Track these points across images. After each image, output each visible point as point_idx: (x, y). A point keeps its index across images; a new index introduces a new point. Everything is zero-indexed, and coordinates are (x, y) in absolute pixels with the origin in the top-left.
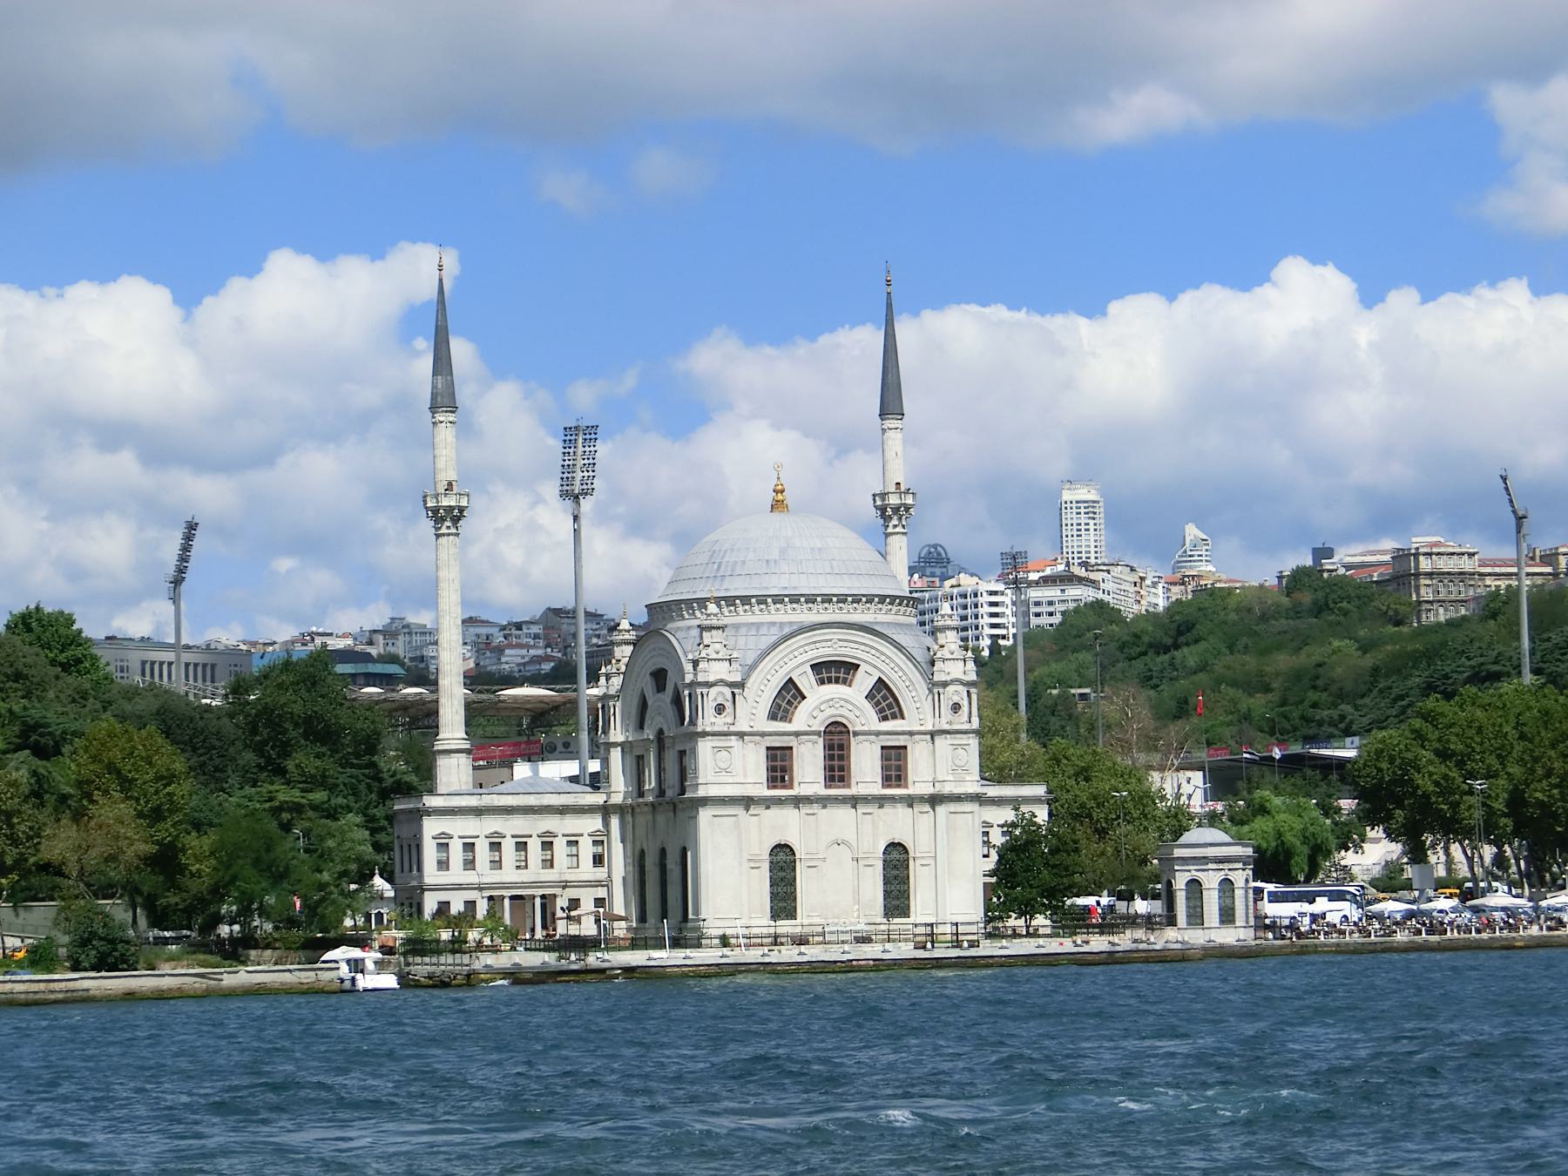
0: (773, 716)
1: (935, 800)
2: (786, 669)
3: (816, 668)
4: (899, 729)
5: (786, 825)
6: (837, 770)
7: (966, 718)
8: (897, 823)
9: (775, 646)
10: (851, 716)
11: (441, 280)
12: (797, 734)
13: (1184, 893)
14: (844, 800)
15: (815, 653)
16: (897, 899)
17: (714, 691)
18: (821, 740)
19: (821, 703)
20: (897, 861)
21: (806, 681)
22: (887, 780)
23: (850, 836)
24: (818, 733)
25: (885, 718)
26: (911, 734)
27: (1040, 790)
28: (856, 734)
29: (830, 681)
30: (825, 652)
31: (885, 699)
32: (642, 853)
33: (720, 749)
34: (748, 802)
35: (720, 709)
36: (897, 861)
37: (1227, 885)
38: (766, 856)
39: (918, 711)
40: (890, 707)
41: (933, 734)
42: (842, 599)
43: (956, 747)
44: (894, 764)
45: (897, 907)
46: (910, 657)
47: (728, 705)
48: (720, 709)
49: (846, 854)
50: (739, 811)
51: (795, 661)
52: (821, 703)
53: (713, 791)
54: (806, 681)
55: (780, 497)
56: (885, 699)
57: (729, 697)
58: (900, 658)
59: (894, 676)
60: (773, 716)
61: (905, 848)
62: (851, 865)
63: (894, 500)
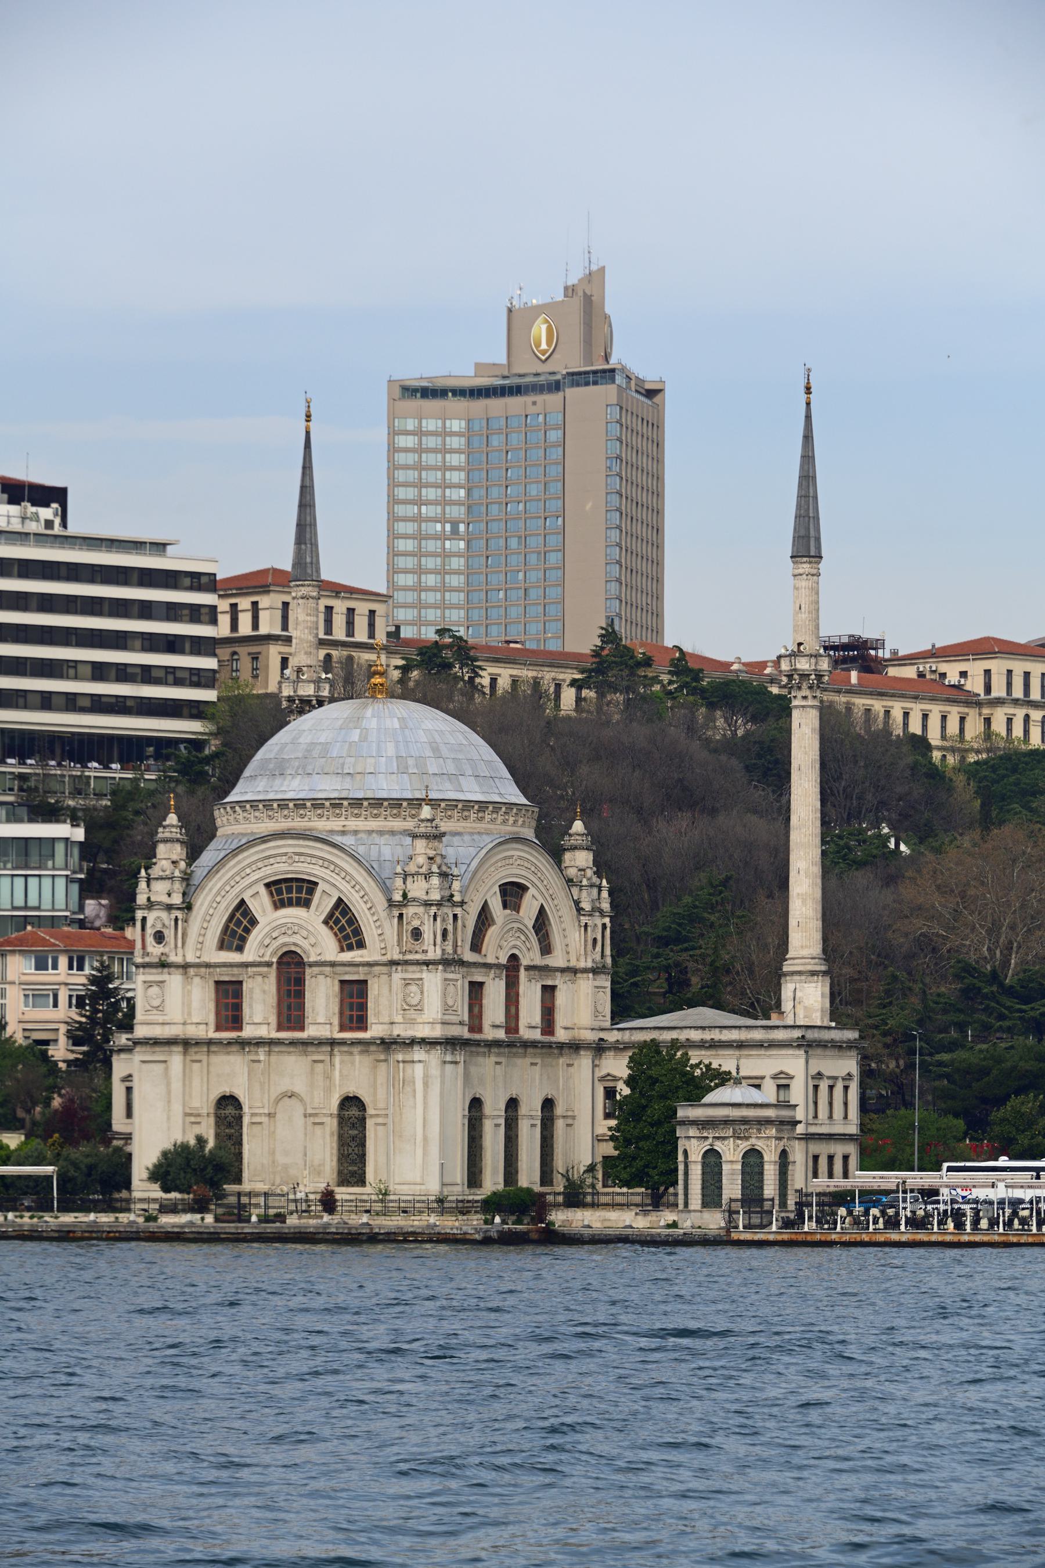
0: (222, 946)
1: (388, 1044)
2: (237, 889)
3: (268, 885)
4: (358, 959)
6: (291, 1008)
9: (221, 863)
10: (304, 944)
11: (308, 433)
12: (246, 965)
13: (699, 1167)
14: (293, 1043)
15: (268, 870)
16: (352, 1164)
18: (273, 972)
19: (275, 927)
21: (260, 905)
23: (299, 1087)
24: (269, 964)
25: (350, 948)
27: (852, 1035)
28: (311, 965)
30: (281, 869)
31: (344, 924)
32: (476, 1104)
33: (148, 984)
34: (186, 1044)
35: (159, 937)
37: (712, 1160)
39: (381, 936)
41: (393, 963)
42: (300, 804)
44: (354, 1001)
45: (353, 1174)
47: (166, 932)
49: (299, 1111)
50: (176, 1059)
54: (260, 905)
56: (344, 924)
58: (360, 876)
60: (222, 946)
61: (364, 1105)
62: (299, 1121)
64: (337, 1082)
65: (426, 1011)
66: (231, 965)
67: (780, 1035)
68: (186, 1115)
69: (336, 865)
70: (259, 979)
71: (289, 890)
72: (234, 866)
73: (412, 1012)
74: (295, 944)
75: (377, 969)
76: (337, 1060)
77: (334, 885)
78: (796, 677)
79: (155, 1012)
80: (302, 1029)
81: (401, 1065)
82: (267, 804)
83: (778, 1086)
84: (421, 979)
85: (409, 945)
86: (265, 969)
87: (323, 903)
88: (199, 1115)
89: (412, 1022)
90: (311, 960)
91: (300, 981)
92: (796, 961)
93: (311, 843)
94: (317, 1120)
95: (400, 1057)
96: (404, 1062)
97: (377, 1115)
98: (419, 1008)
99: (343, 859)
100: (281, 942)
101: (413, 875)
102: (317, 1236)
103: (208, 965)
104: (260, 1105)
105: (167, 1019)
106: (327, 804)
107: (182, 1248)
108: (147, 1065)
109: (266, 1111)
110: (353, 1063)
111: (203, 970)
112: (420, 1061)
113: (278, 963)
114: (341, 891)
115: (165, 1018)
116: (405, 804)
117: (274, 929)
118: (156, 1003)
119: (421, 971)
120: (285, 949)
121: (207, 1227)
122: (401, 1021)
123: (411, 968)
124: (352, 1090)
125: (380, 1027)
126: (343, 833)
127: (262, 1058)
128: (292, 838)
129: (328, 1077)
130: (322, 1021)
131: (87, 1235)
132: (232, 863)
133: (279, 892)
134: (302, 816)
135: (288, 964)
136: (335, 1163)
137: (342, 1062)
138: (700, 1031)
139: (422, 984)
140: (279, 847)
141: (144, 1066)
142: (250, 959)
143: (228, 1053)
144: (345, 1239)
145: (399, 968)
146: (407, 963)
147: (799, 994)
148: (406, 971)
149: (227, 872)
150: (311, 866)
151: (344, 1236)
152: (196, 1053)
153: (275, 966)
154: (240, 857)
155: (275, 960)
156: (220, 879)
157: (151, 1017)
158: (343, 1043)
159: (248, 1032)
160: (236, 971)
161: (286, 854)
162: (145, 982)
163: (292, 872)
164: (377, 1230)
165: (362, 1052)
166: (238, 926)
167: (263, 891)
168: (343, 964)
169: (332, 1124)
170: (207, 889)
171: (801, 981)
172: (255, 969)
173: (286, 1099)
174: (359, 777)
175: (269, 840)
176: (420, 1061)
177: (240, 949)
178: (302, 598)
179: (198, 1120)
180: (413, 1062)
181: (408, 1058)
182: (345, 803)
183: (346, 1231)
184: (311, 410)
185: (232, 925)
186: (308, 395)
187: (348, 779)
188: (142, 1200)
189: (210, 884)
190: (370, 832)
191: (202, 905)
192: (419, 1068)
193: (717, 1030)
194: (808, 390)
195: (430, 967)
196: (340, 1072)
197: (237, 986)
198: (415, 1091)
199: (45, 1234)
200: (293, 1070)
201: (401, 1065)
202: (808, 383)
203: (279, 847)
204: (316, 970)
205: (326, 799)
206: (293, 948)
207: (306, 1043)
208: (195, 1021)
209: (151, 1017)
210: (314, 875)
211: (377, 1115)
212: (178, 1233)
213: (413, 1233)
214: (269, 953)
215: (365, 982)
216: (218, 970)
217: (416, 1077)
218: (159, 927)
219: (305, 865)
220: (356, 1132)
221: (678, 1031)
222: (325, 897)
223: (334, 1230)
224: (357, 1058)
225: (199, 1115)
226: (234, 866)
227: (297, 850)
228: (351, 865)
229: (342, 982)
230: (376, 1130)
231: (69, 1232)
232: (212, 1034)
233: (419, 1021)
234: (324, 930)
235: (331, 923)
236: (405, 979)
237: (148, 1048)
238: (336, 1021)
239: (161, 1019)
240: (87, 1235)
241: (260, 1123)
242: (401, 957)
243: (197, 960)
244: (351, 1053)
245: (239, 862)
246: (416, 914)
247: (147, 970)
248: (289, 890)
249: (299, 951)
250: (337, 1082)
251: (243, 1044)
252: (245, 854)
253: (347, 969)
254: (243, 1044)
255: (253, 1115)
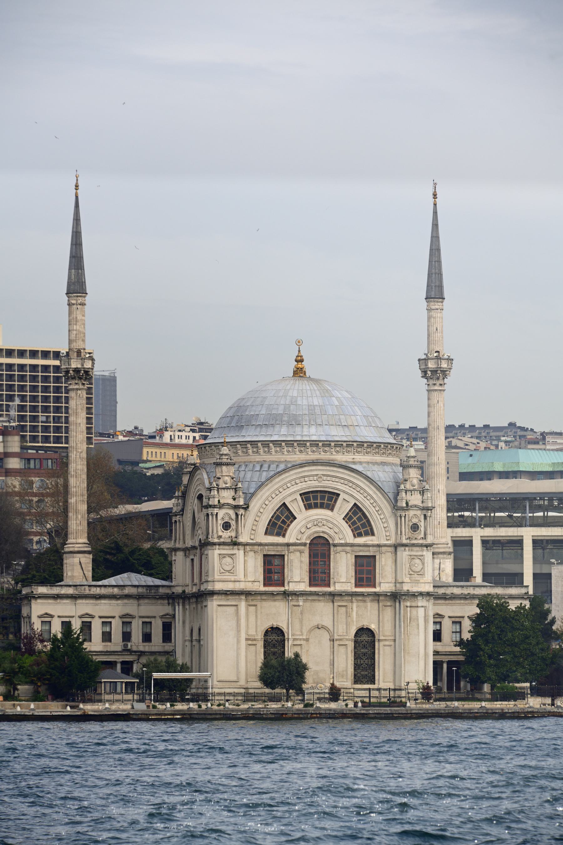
2: (281, 497)
4: (370, 543)
5: (277, 613)
6: (319, 572)
7: (422, 535)
8: (366, 615)
10: (331, 532)
11: (77, 197)
12: (288, 545)
14: (324, 594)
15: (304, 485)
16: (365, 669)
17: (221, 513)
19: (307, 523)
20: (365, 643)
22: (359, 582)
23: (328, 622)
24: (305, 544)
25: (360, 535)
26: (379, 546)
29: (316, 506)
30: (312, 485)
31: (359, 520)
35: (226, 526)
36: (365, 643)
38: (260, 636)
40: (363, 526)
42: (327, 444)
43: (412, 558)
44: (365, 570)
46: (379, 489)
47: (233, 523)
48: (226, 526)
51: (287, 490)
52: (307, 523)
53: (218, 586)
55: (300, 366)
56: (359, 520)
57: (233, 516)
58: (371, 490)
59: (367, 503)
62: (328, 644)
63: (431, 365)
64: (355, 619)
65: (426, 575)
66: (277, 545)
67: (64, 591)
68: (247, 639)
69: (353, 483)
70: (298, 554)
71: (315, 498)
72: (279, 482)
73: (416, 576)
74: (323, 532)
75: (384, 549)
76: (355, 605)
77: (352, 496)
78: (429, 372)
79: (227, 574)
80: (329, 585)
81: (409, 609)
82: (290, 443)
83: (123, 623)
84: (422, 556)
85: (410, 534)
86: (303, 547)
87: (343, 507)
88: (255, 640)
89: (417, 582)
90: (336, 542)
91: (327, 557)
92: (439, 546)
93: (335, 469)
94: (341, 643)
95: (408, 604)
96: (411, 607)
97: (385, 640)
98: (421, 573)
99: (358, 479)
100: (314, 530)
101: (411, 491)
102: (463, 715)
103: (260, 545)
104: (300, 633)
105: (236, 578)
106: (345, 444)
107: (539, 721)
108: (221, 607)
109: (304, 637)
110: (366, 607)
111: (256, 547)
112: (422, 606)
113: (310, 544)
114: (357, 500)
115: (236, 577)
116: (283, 444)
117: (308, 523)
118: (228, 568)
119: (423, 551)
120: (316, 535)
121: (350, 710)
122: (409, 581)
123: (415, 549)
124: (365, 623)
125: (387, 585)
126: (354, 463)
127: (301, 603)
128: (322, 465)
129: (348, 615)
130: (345, 581)
131: (296, 716)
132: (277, 480)
133: (308, 499)
134: (325, 451)
135: (317, 544)
136: (353, 670)
137: (357, 607)
138: (460, 589)
139: (424, 559)
140: (311, 470)
141: (219, 608)
142: (292, 541)
143: (275, 600)
144: (483, 716)
145: (407, 548)
146: (413, 545)
147: (442, 566)
148: (412, 550)
149: (273, 485)
150: (335, 483)
151: (482, 714)
152: (252, 600)
153: (308, 545)
154: (283, 476)
155: (308, 542)
156: (268, 490)
157: (224, 577)
158: (362, 594)
159: (292, 587)
160: (279, 548)
161: (317, 475)
162: (220, 554)
163: (324, 487)
164: (507, 711)
165: (372, 601)
166: (281, 520)
167: (299, 498)
168: (359, 545)
169: (351, 645)
170: (259, 496)
171: (444, 558)
172: (294, 547)
173: (317, 629)
174: (351, 428)
175: (305, 466)
176: (422, 606)
177: (284, 536)
178: (80, 305)
179: (254, 642)
180: (417, 607)
181: (414, 604)
182: (355, 444)
183: (485, 711)
184: (79, 182)
185: (273, 519)
186: (78, 173)
187: (346, 429)
188: (219, 694)
189: (261, 493)
190: (368, 463)
191: (255, 506)
192: (421, 611)
193: (472, 588)
194: (435, 196)
195: (429, 548)
196: (357, 613)
197: (372, 559)
198: (418, 625)
199: (264, 716)
200: (322, 612)
201: (409, 609)
202: (435, 192)
203: (311, 470)
204: (339, 548)
205: (345, 441)
206: (322, 535)
207: (333, 595)
208: (250, 580)
209: (224, 577)
210: (337, 489)
211: (385, 640)
212: (364, 714)
213: (531, 712)
214: (305, 538)
215: (374, 557)
216: (266, 547)
217: (419, 616)
218: (227, 519)
219: (331, 482)
220: (367, 650)
221: (445, 588)
222: (345, 502)
223: (477, 711)
224: (369, 604)
225: (255, 640)
226: (279, 482)
227: (325, 473)
228: (364, 483)
229: (356, 556)
230: (384, 650)
231: (283, 714)
232: (262, 588)
233: (421, 581)
234: (343, 523)
235: (346, 519)
236: (410, 555)
237: (223, 597)
238: (353, 581)
239: (233, 578)
240: (296, 716)
241: (300, 645)
242: (408, 541)
243: (251, 541)
244: (365, 601)
245: (283, 479)
246: (415, 515)
247: (221, 547)
248: (323, 498)
249: (326, 536)
250: (355, 619)
251: (286, 595)
252: (287, 474)
253: (361, 548)
254: (286, 595)
255: (294, 640)
